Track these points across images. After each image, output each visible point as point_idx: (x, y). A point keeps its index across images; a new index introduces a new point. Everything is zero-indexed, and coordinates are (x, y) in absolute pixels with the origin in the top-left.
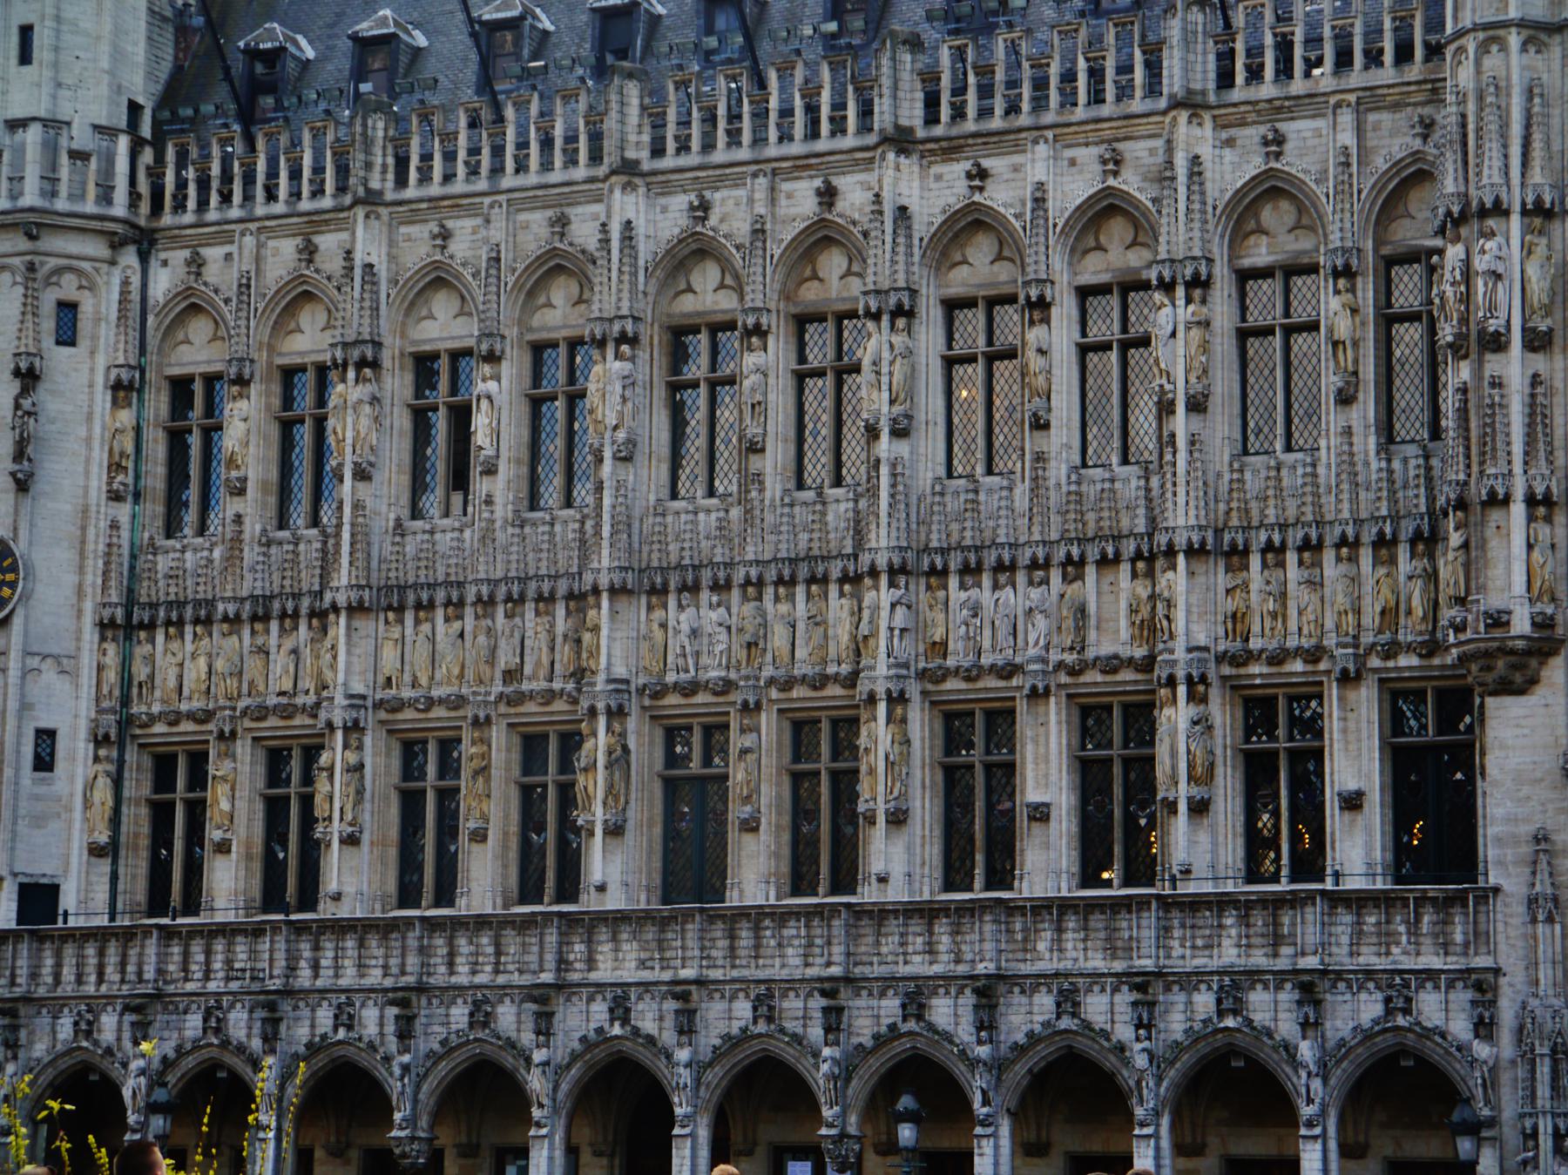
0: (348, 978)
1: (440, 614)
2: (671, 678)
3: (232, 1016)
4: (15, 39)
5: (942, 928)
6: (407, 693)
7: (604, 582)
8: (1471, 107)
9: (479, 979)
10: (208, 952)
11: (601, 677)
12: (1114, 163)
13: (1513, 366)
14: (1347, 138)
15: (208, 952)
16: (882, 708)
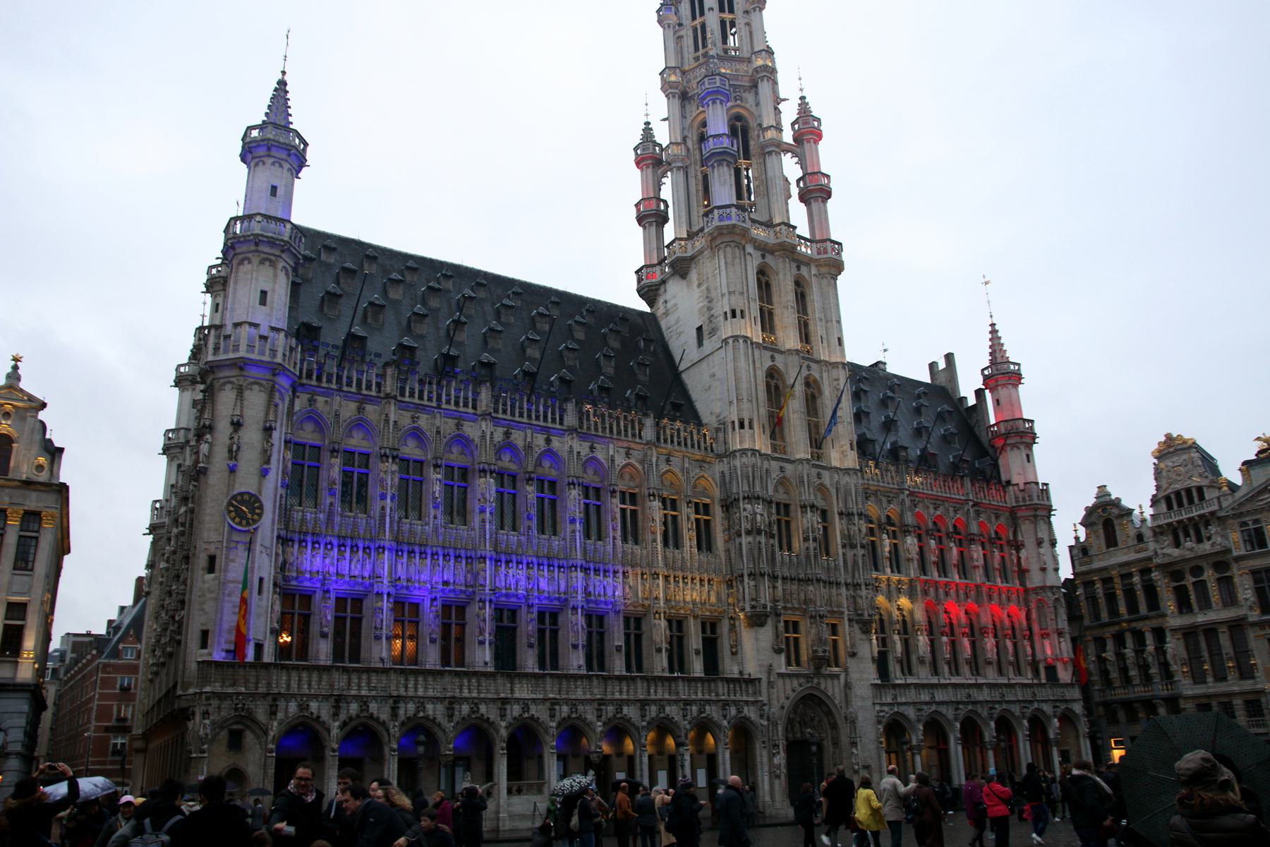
0: (421, 692)
1: (418, 555)
2: (504, 591)
3: (371, 705)
4: (259, 294)
5: (624, 685)
6: (405, 584)
7: (488, 554)
8: (750, 469)
9: (475, 695)
10: (360, 679)
11: (487, 588)
12: (628, 454)
13: (763, 539)
14: (687, 465)
15: (360, 679)
16: (580, 610)
